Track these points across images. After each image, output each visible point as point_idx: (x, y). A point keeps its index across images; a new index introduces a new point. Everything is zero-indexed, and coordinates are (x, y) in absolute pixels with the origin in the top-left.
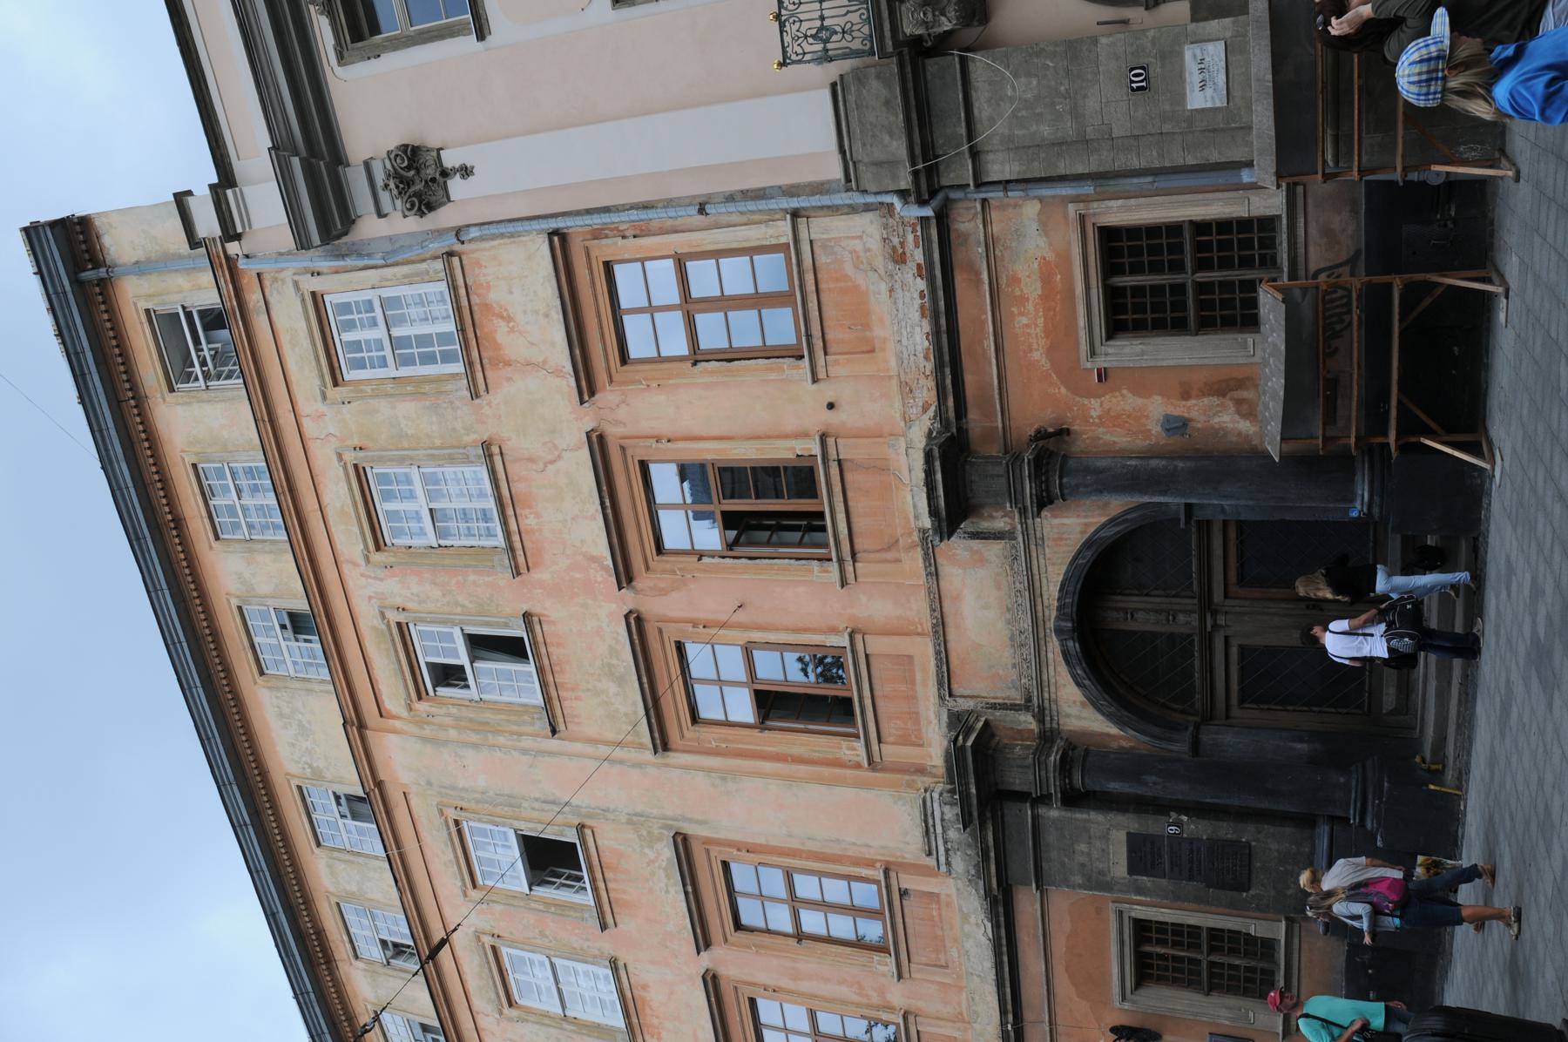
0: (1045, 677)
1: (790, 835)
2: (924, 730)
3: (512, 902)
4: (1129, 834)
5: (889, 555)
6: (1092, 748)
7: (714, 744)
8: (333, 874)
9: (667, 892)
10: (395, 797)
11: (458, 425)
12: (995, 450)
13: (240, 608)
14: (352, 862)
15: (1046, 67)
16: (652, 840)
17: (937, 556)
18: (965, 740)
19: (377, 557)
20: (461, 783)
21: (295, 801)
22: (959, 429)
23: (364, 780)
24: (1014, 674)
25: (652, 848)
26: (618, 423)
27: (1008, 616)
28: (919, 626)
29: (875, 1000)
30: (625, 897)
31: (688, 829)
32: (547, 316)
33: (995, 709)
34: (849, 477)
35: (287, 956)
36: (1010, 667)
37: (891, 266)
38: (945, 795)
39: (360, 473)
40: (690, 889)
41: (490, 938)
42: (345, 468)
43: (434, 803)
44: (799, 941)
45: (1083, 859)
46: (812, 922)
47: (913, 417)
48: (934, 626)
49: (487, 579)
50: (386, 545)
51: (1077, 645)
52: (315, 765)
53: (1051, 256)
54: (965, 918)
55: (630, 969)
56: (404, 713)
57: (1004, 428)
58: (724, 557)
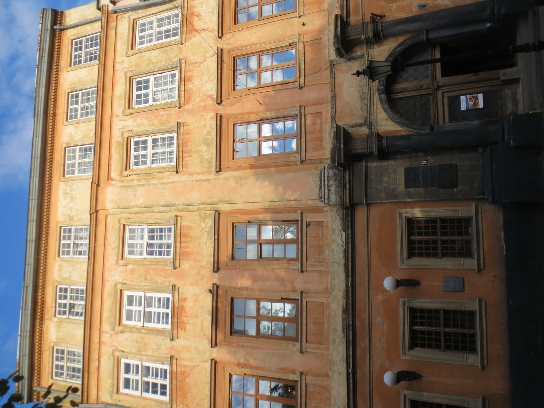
4: (405, 169)
8: (60, 270)
9: (206, 244)
11: (172, 56)
17: (335, 71)
20: (132, 204)
22: (347, 20)
23: (92, 208)
24: (360, 112)
25: (204, 222)
30: (187, 250)
32: (212, 13)
36: (359, 109)
40: (216, 237)
41: (122, 285)
42: (126, 79)
43: (117, 218)
45: (385, 185)
50: (132, 108)
51: (385, 96)
55: (181, 290)
57: (362, 18)
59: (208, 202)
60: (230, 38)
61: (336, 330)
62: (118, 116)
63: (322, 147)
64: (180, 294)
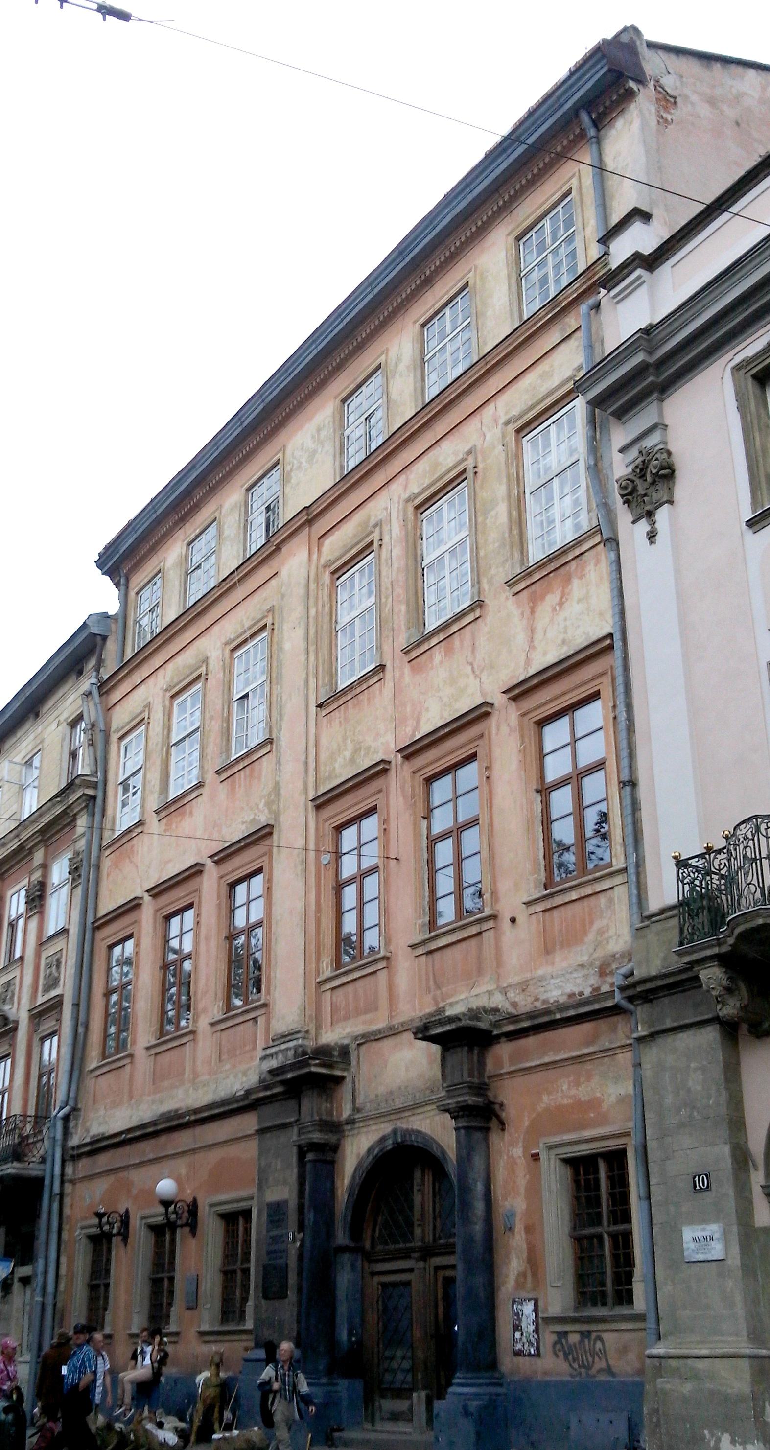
0: (371, 1122)
5: (431, 983)
6: (336, 1166)
9: (243, 823)
11: (493, 571)
12: (490, 1068)
15: (709, 1098)
16: (268, 804)
22: (498, 1037)
29: (201, 1006)
37: (597, 963)
38: (300, 1049)
43: (275, 603)
44: (227, 938)
48: (394, 1026)
51: (390, 1147)
53: (605, 1106)
54: (245, 1074)
56: (322, 561)
61: (162, 1102)
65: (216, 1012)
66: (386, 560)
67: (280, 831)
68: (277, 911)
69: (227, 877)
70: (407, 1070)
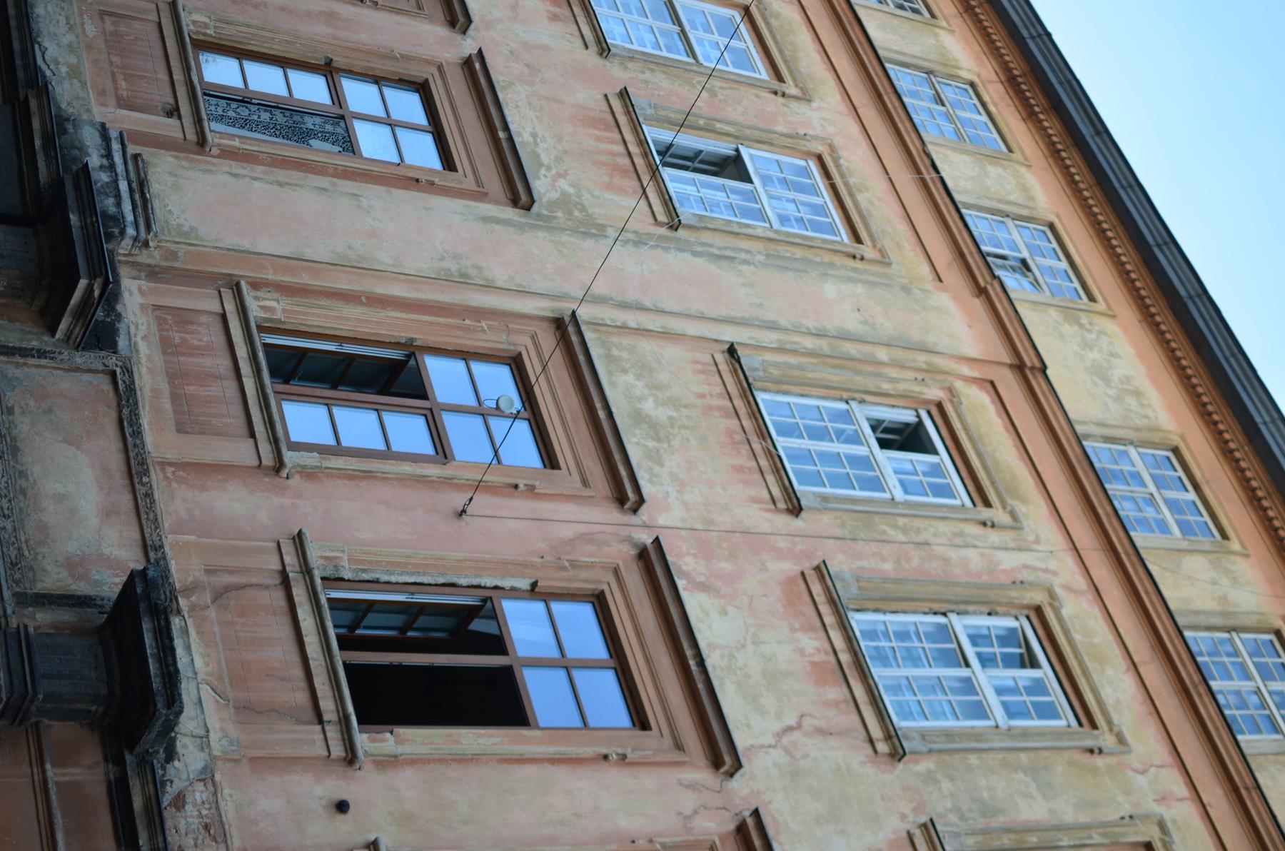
1: (355, 196)
2: (154, 329)
3: (762, 134)
7: (484, 324)
8: (1025, 189)
9: (534, 135)
10: (953, 276)
11: (946, 786)
12: (57, 730)
13: (1225, 536)
14: (999, 201)
16: (564, 202)
18: (90, 288)
19: (1038, 598)
20: (860, 289)
21: (1095, 282)
22: (120, 762)
25: (564, 194)
26: (692, 786)
27: (23, 483)
28: (169, 475)
30: (597, 133)
31: (510, 213)
33: (39, 351)
34: (302, 697)
35: (1069, 82)
38: (116, 231)
39: (1086, 717)
40: (502, 135)
41: (787, 91)
42: (1110, 723)
43: (894, 266)
44: (329, 63)
46: (311, 89)
47: (200, 786)
48: (146, 473)
49: (864, 563)
50: (1028, 617)
52: (1076, 328)
54: (75, 72)
55: (579, 42)
56: (959, 385)
57: (42, 764)
58: (496, 588)
59: (570, 235)
60: (696, 812)
62: (1068, 588)
63: (161, 322)
64: (577, 33)
65: (196, 17)
66: (960, 534)
67: (520, 227)
68: (375, 195)
69: (439, 81)
70: (60, 498)
